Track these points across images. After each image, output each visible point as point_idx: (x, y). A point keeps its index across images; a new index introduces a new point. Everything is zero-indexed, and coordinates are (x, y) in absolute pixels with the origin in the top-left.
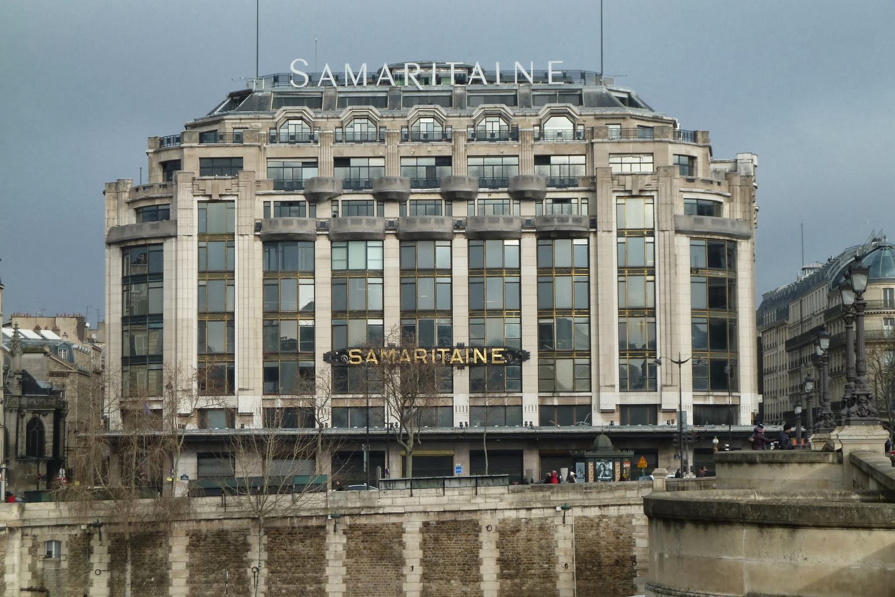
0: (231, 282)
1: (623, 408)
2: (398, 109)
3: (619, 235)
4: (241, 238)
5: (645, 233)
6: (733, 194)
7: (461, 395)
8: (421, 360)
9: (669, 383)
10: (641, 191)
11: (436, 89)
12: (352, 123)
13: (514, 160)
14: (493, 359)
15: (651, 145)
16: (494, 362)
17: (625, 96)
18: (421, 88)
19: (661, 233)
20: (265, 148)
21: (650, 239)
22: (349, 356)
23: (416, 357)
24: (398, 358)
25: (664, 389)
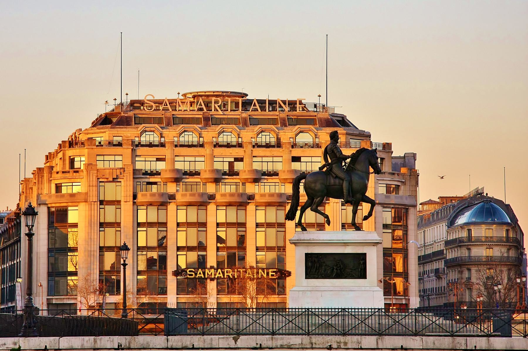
0: (118, 229)
2: (209, 127)
3: (342, 206)
4: (125, 203)
6: (405, 181)
8: (228, 276)
12: (183, 134)
13: (280, 159)
16: (270, 277)
18: (221, 113)
20: (135, 150)
22: (187, 273)
23: (226, 274)
24: (215, 275)
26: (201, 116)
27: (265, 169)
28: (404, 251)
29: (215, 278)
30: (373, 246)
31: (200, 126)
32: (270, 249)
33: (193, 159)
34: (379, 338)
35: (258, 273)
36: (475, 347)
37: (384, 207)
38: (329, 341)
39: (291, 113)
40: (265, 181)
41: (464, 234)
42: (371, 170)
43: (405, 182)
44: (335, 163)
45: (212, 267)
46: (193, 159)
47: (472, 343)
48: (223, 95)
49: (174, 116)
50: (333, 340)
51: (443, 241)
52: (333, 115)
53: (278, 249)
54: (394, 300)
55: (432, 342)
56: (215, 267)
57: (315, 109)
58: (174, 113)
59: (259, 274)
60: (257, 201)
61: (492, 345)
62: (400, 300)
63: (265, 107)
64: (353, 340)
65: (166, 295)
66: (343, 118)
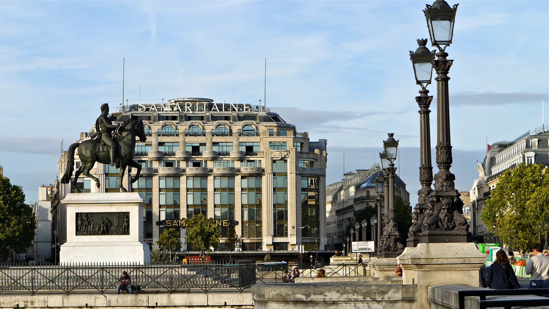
9: (293, 234)
11: (198, 113)
12: (165, 127)
18: (191, 112)
21: (286, 177)
26: (177, 115)
27: (221, 151)
28: (316, 207)
29: (185, 226)
30: (136, 205)
31: (177, 122)
32: (222, 206)
33: (171, 144)
34: (65, 297)
36: (157, 303)
37: (302, 177)
38: (16, 300)
39: (240, 112)
40: (221, 159)
41: (364, 194)
42: (137, 138)
43: (317, 159)
44: (104, 132)
45: (183, 219)
46: (171, 144)
47: (154, 300)
48: (194, 101)
49: (159, 115)
50: (20, 300)
51: (352, 199)
52: (269, 114)
54: (309, 240)
55: (116, 299)
57: (257, 110)
58: (159, 113)
60: (214, 173)
61: (173, 301)
63: (222, 108)
64: (39, 299)
65: (152, 238)
66: (276, 115)
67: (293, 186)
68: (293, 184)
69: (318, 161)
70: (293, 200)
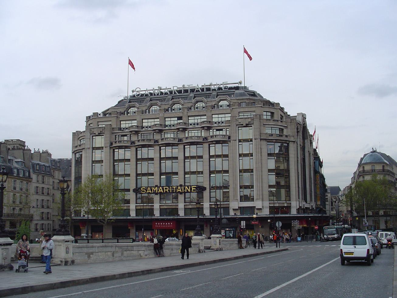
1: (240, 208)
4: (105, 148)
5: (249, 140)
6: (287, 126)
7: (181, 204)
8: (167, 191)
9: (259, 198)
10: (247, 124)
14: (192, 190)
15: (255, 108)
17: (253, 94)
18: (178, 94)
19: (255, 140)
20: (119, 117)
23: (165, 190)
24: (158, 191)
25: (257, 200)
35: (185, 189)
37: (268, 142)
45: (156, 186)
53: (198, 173)
56: (159, 186)
58: (152, 97)
59: (185, 189)
62: (282, 204)
66: (254, 93)
67: (257, 152)
68: (257, 149)
69: (288, 128)
70: (258, 164)
